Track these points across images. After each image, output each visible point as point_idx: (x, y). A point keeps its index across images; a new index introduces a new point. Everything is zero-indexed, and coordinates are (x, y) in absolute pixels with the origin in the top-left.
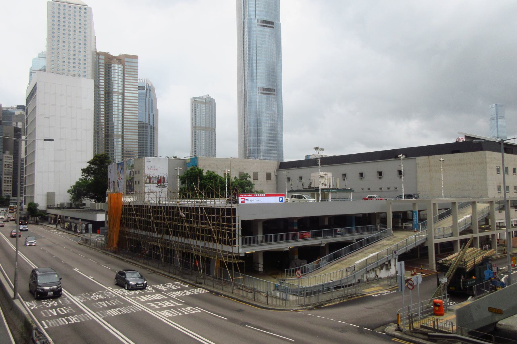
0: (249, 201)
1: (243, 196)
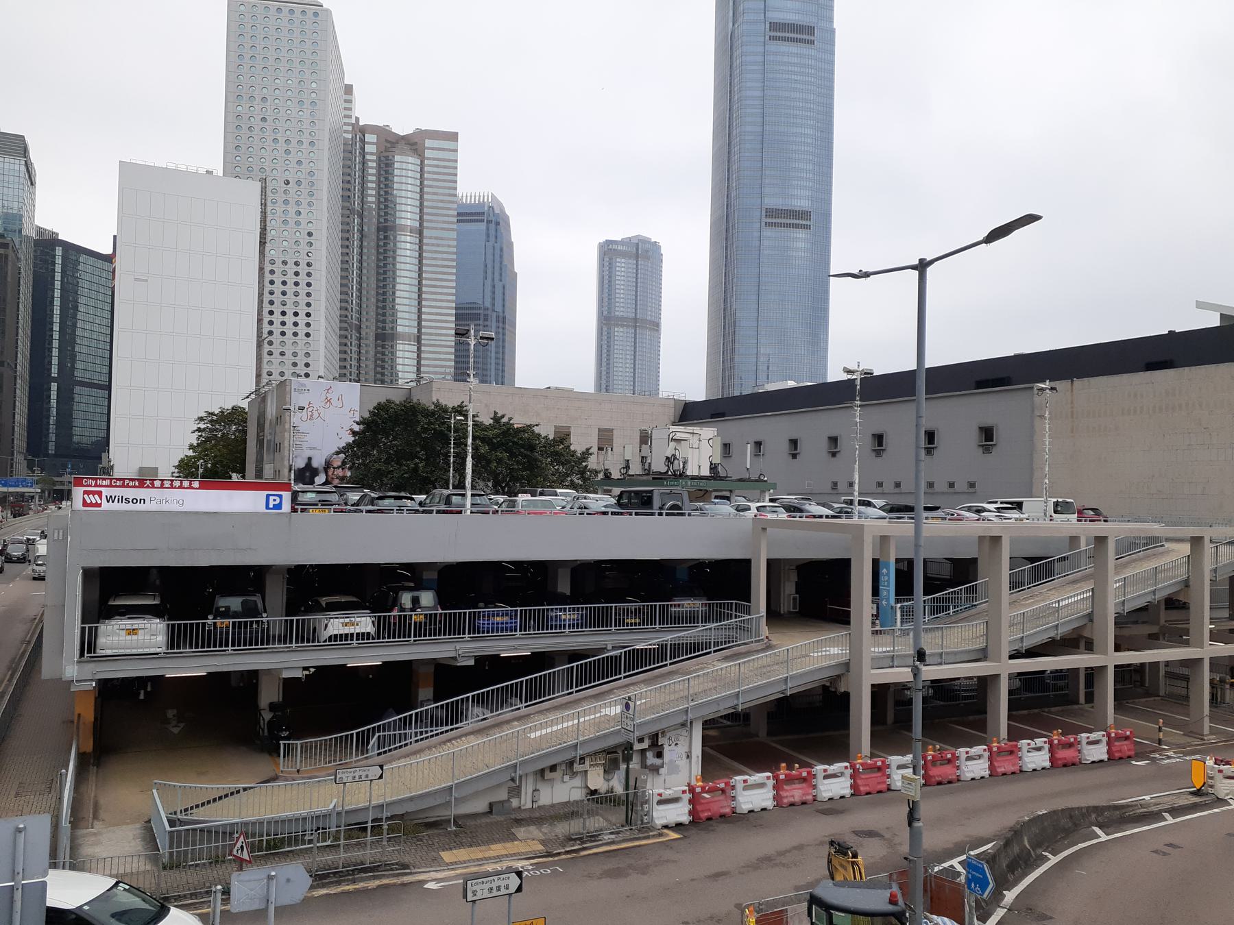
0: (121, 500)
1: (96, 485)
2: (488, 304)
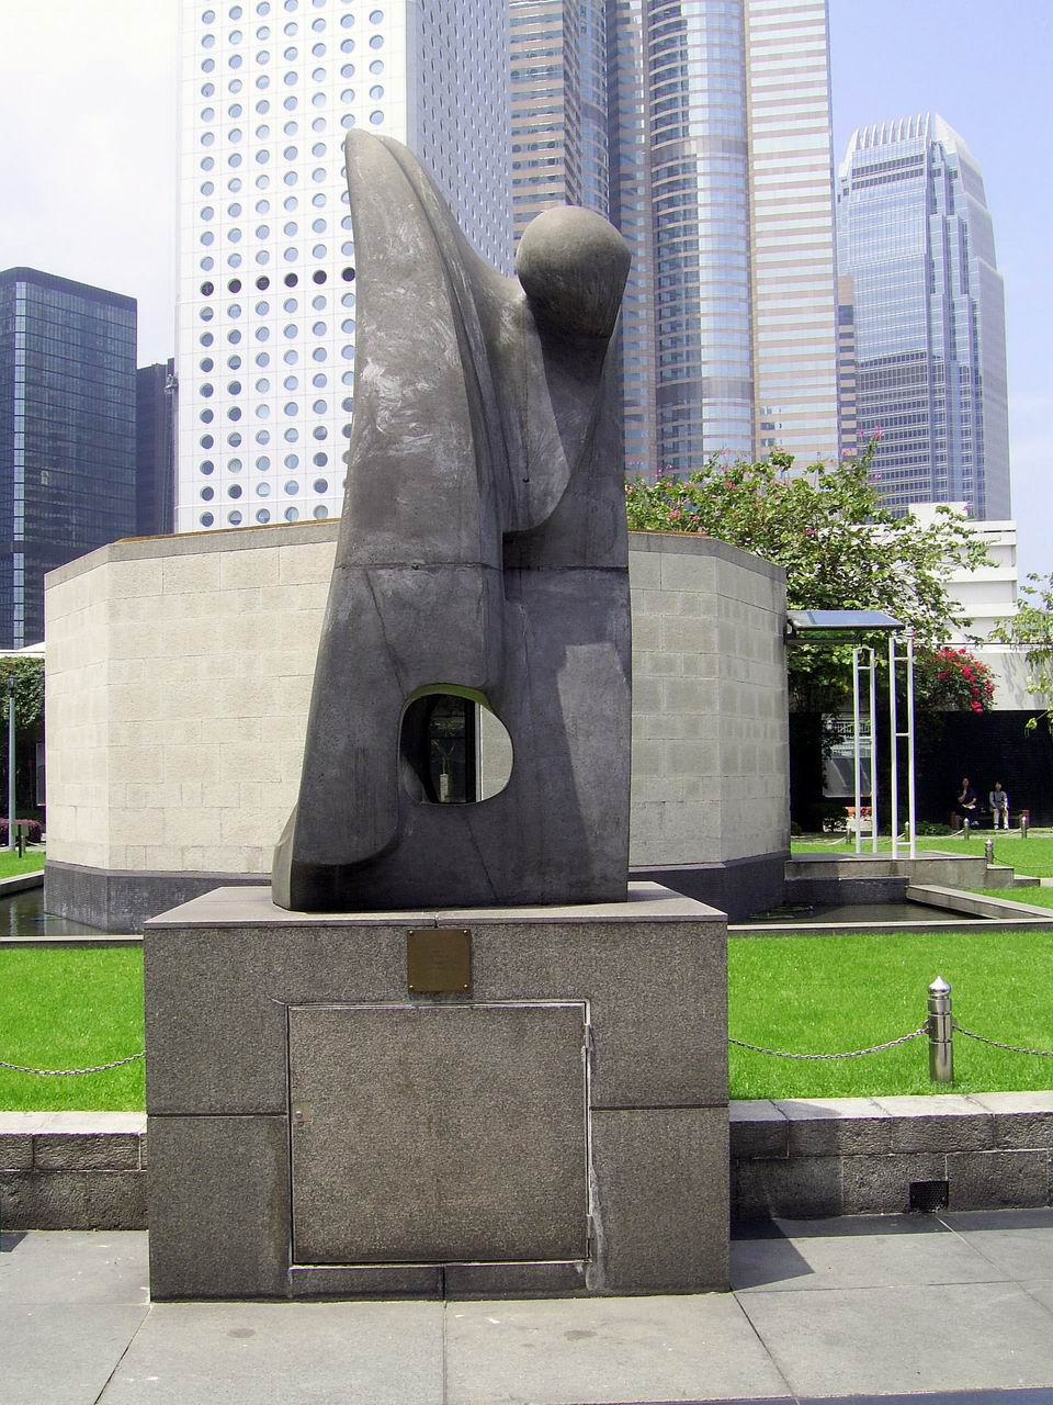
2: (939, 349)
